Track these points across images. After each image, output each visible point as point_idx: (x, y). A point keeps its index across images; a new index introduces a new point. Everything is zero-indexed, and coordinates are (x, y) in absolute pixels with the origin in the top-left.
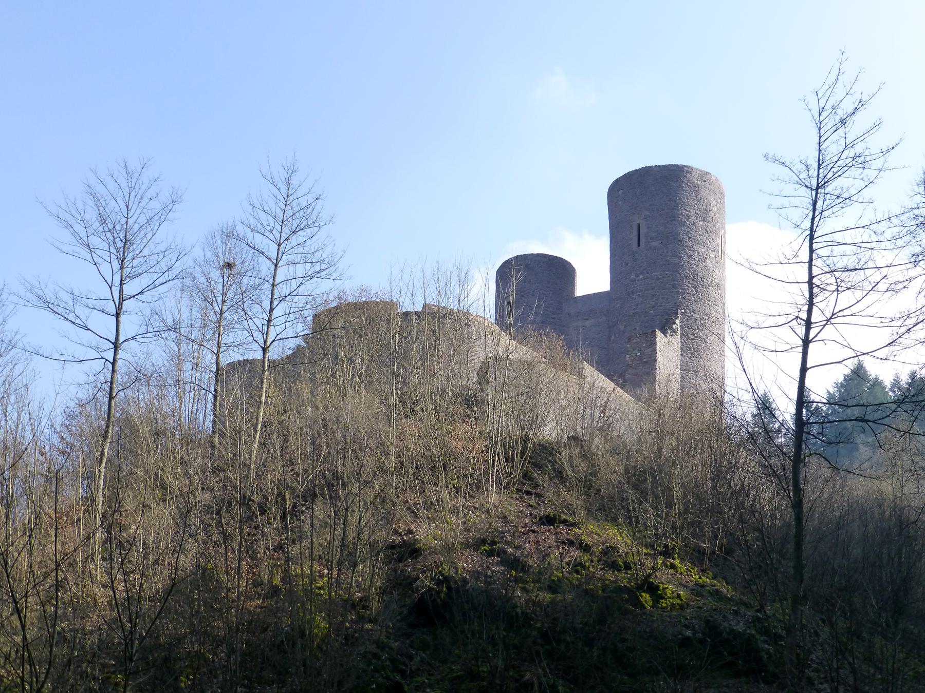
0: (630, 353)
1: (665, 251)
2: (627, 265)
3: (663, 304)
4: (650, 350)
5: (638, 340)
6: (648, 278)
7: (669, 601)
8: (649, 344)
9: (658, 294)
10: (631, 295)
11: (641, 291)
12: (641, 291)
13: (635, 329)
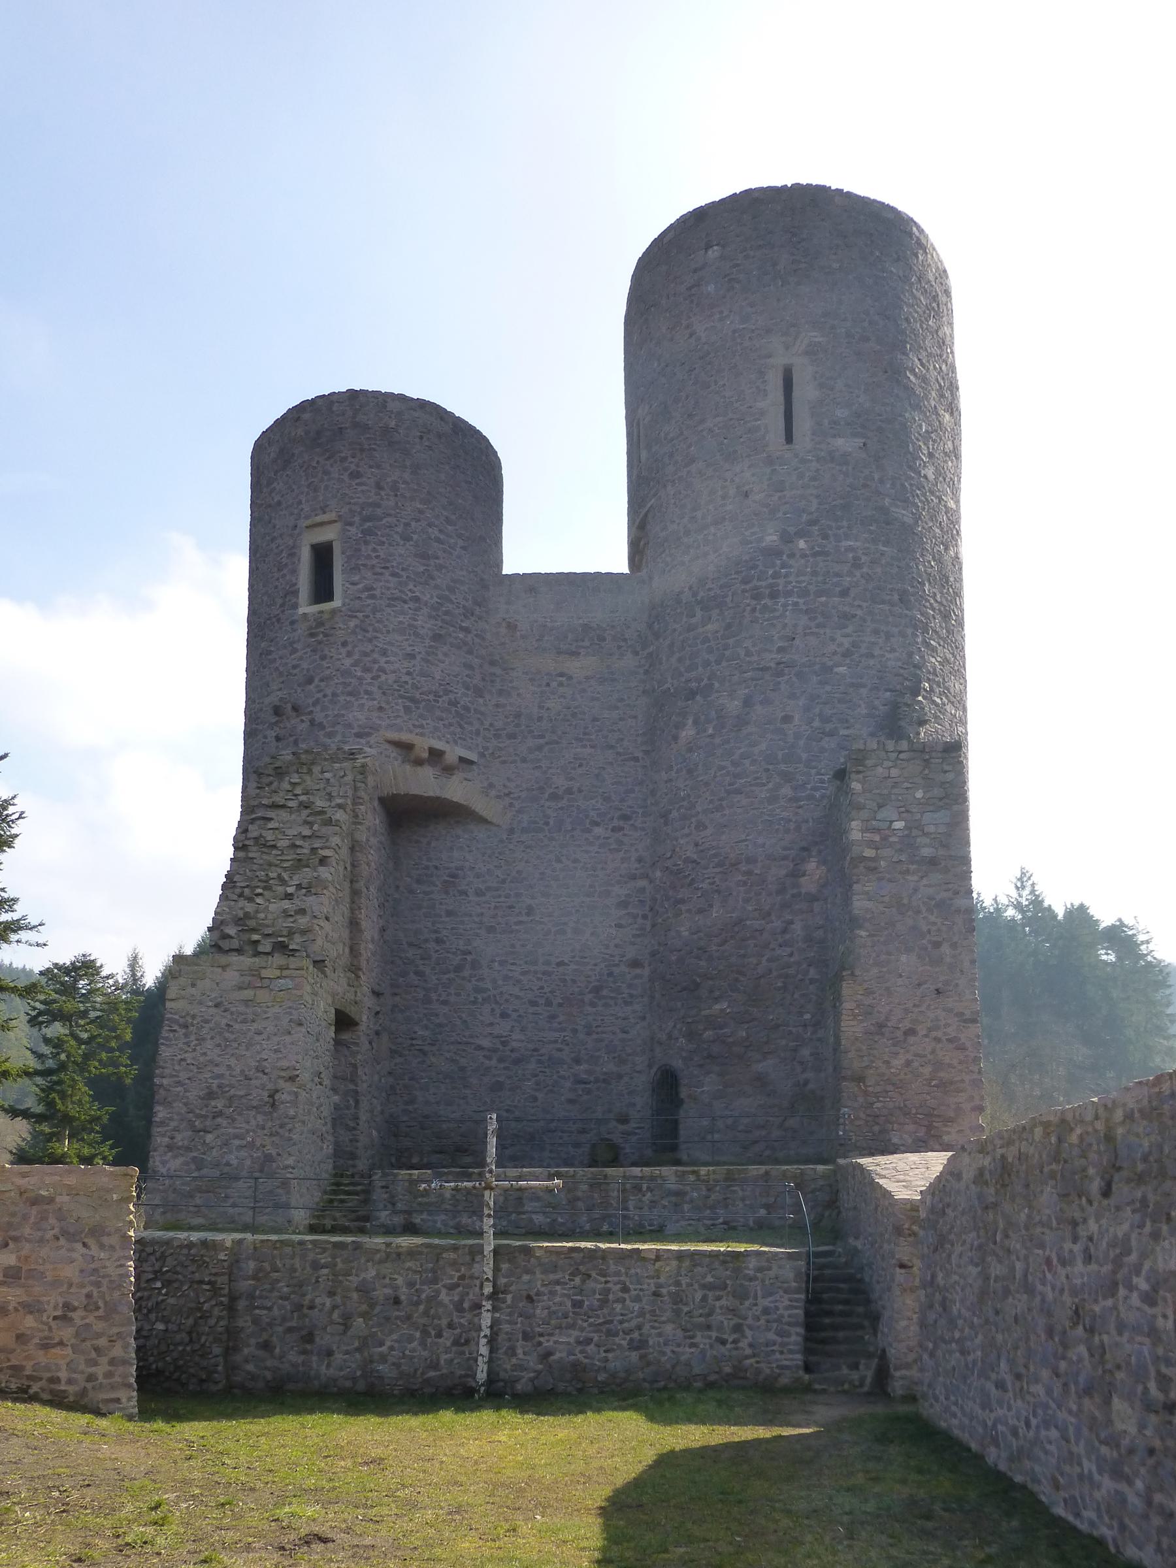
0: (865, 814)
1: (876, 477)
2: (746, 495)
3: (877, 652)
4: (942, 816)
5: (894, 772)
6: (826, 554)
7: (452, 1277)
8: (937, 792)
9: (859, 612)
10: (766, 601)
11: (804, 593)
12: (804, 593)
13: (787, 719)
